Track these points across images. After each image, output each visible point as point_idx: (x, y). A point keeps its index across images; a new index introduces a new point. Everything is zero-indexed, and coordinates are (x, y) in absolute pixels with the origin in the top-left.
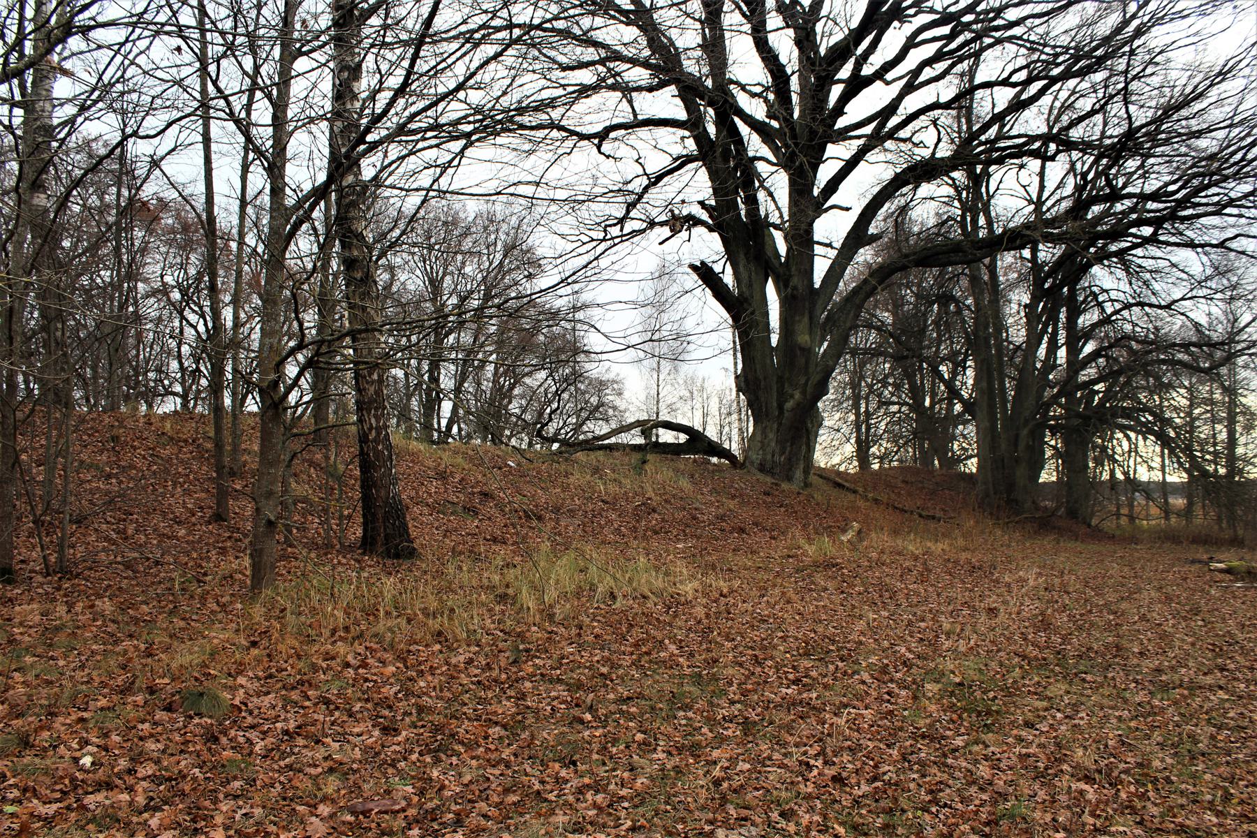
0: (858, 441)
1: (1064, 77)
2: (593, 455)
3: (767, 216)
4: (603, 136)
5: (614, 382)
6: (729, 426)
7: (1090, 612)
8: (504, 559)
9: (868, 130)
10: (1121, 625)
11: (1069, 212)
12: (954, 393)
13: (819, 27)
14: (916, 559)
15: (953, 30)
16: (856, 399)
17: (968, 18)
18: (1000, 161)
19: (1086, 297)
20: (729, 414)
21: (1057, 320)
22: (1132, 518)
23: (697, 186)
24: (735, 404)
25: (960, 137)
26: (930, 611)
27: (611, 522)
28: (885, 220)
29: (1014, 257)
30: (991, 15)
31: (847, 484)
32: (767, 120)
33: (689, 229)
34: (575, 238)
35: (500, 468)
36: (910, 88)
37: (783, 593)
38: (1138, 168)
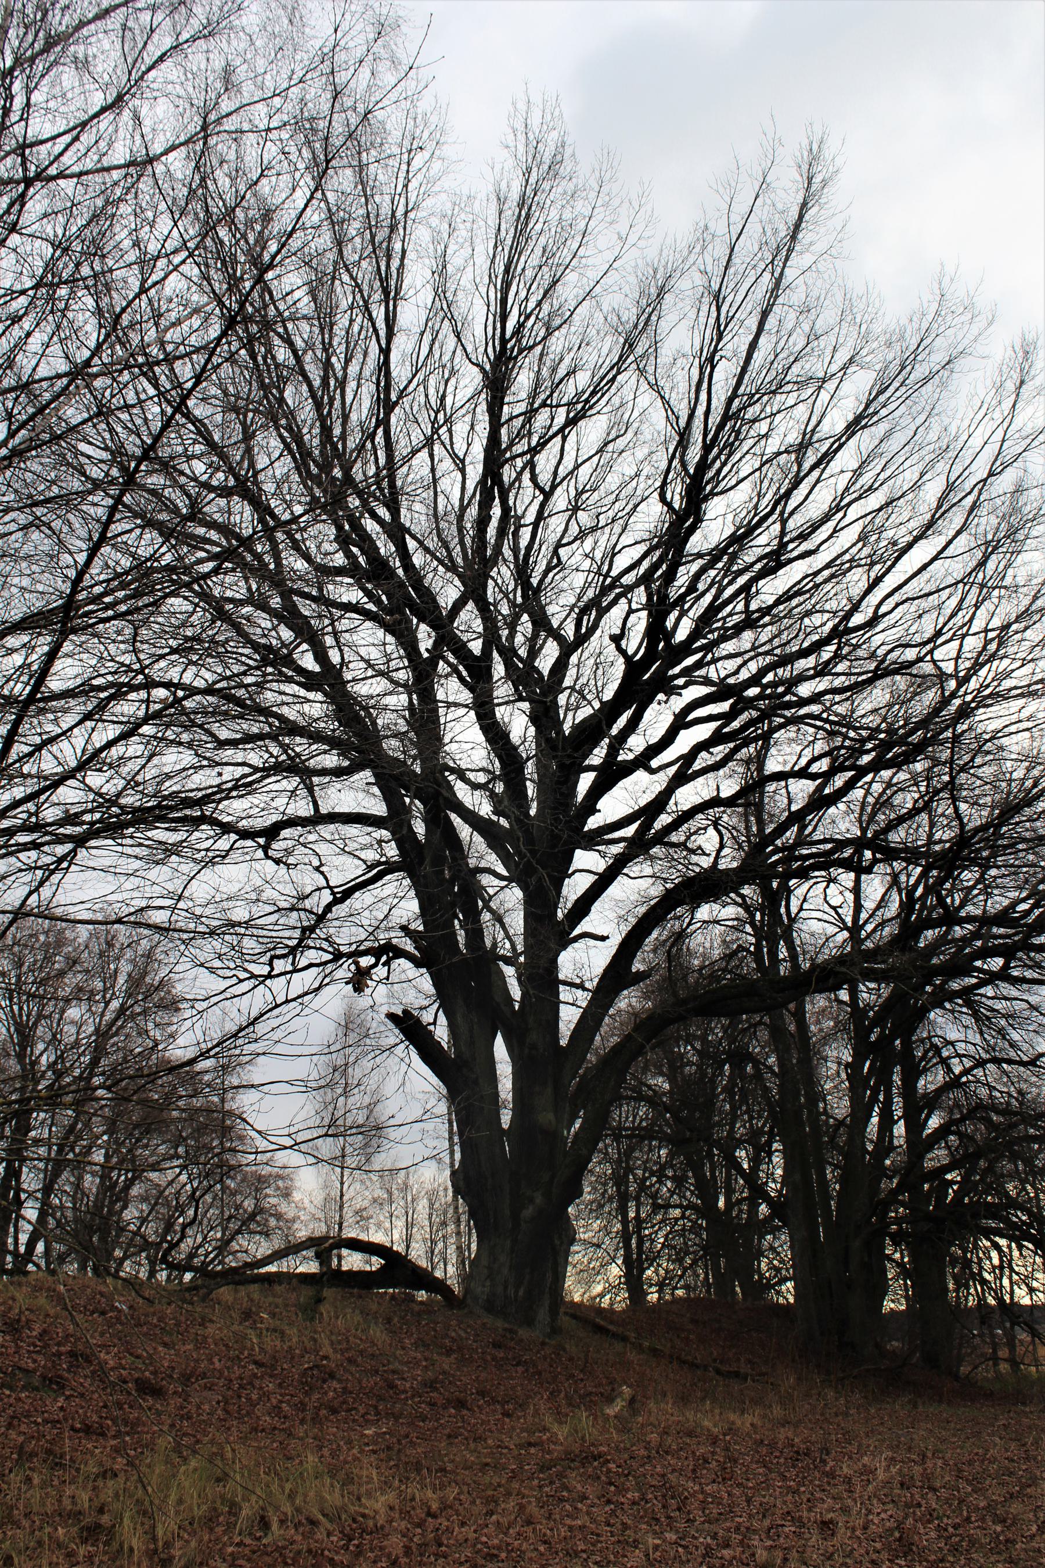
0: (627, 1261)
1: (875, 767)
2: (243, 1291)
3: (495, 945)
4: (272, 832)
5: (279, 1177)
6: (445, 1253)
7: (968, 1520)
8: (101, 1464)
9: (629, 831)
10: (1013, 1542)
11: (895, 941)
12: (758, 1192)
13: (562, 699)
14: (715, 1441)
15: (732, 706)
16: (623, 1199)
17: (753, 692)
18: (803, 874)
19: (926, 1052)
20: (444, 1224)
21: (889, 1085)
22: (1014, 1363)
23: (398, 903)
24: (451, 1211)
25: (749, 841)
26: (737, 1529)
27: (266, 1395)
28: (654, 951)
29: (829, 1000)
30: (780, 689)
31: (611, 1327)
32: (495, 818)
33: (387, 963)
34: (230, 973)
35: (103, 1313)
36: (681, 778)
37: (522, 1507)
38: (978, 882)
